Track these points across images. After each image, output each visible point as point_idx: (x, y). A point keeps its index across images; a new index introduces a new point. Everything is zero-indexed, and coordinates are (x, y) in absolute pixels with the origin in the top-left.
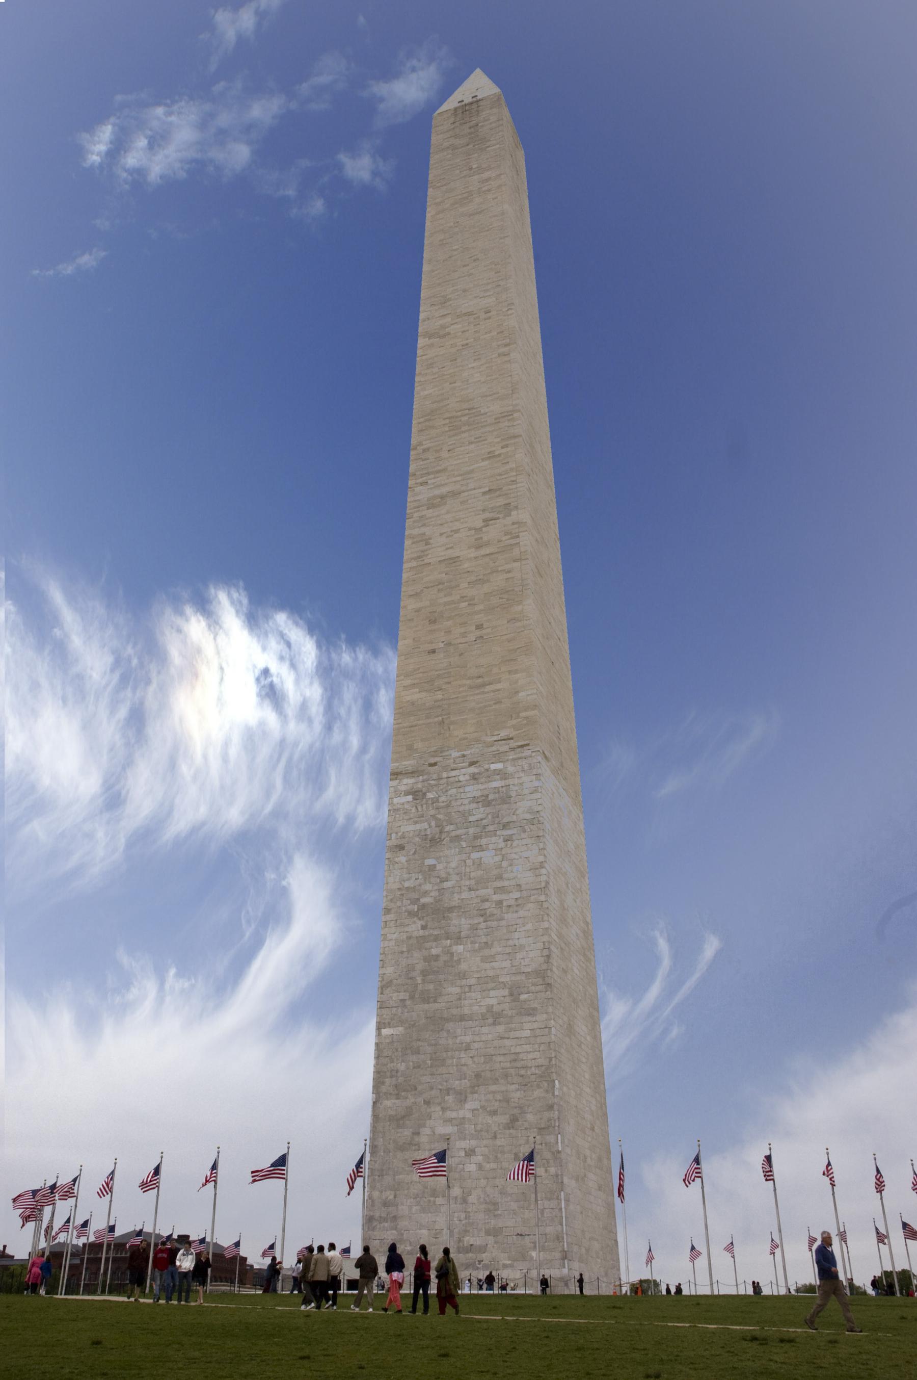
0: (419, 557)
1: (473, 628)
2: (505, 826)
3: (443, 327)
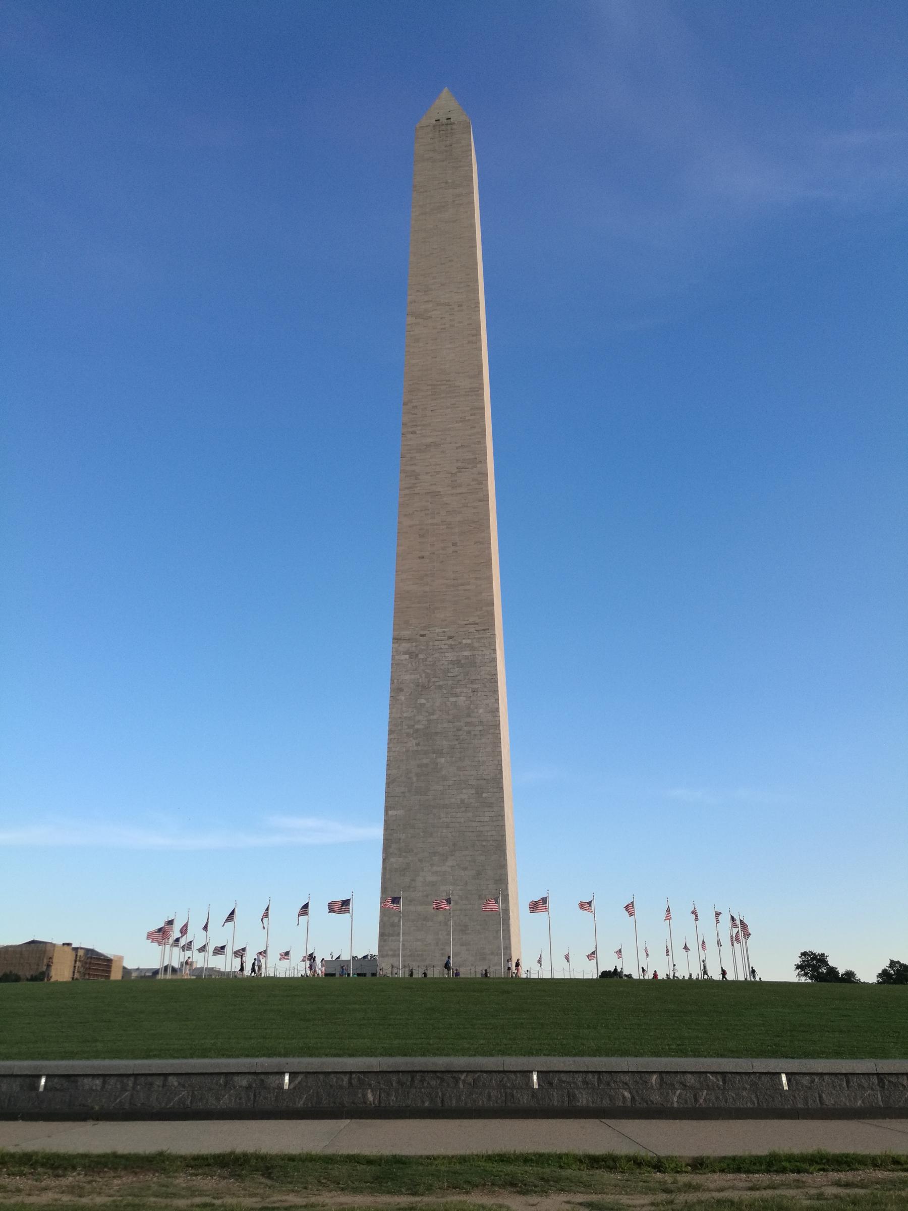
0: (410, 488)
1: (450, 544)
2: (473, 682)
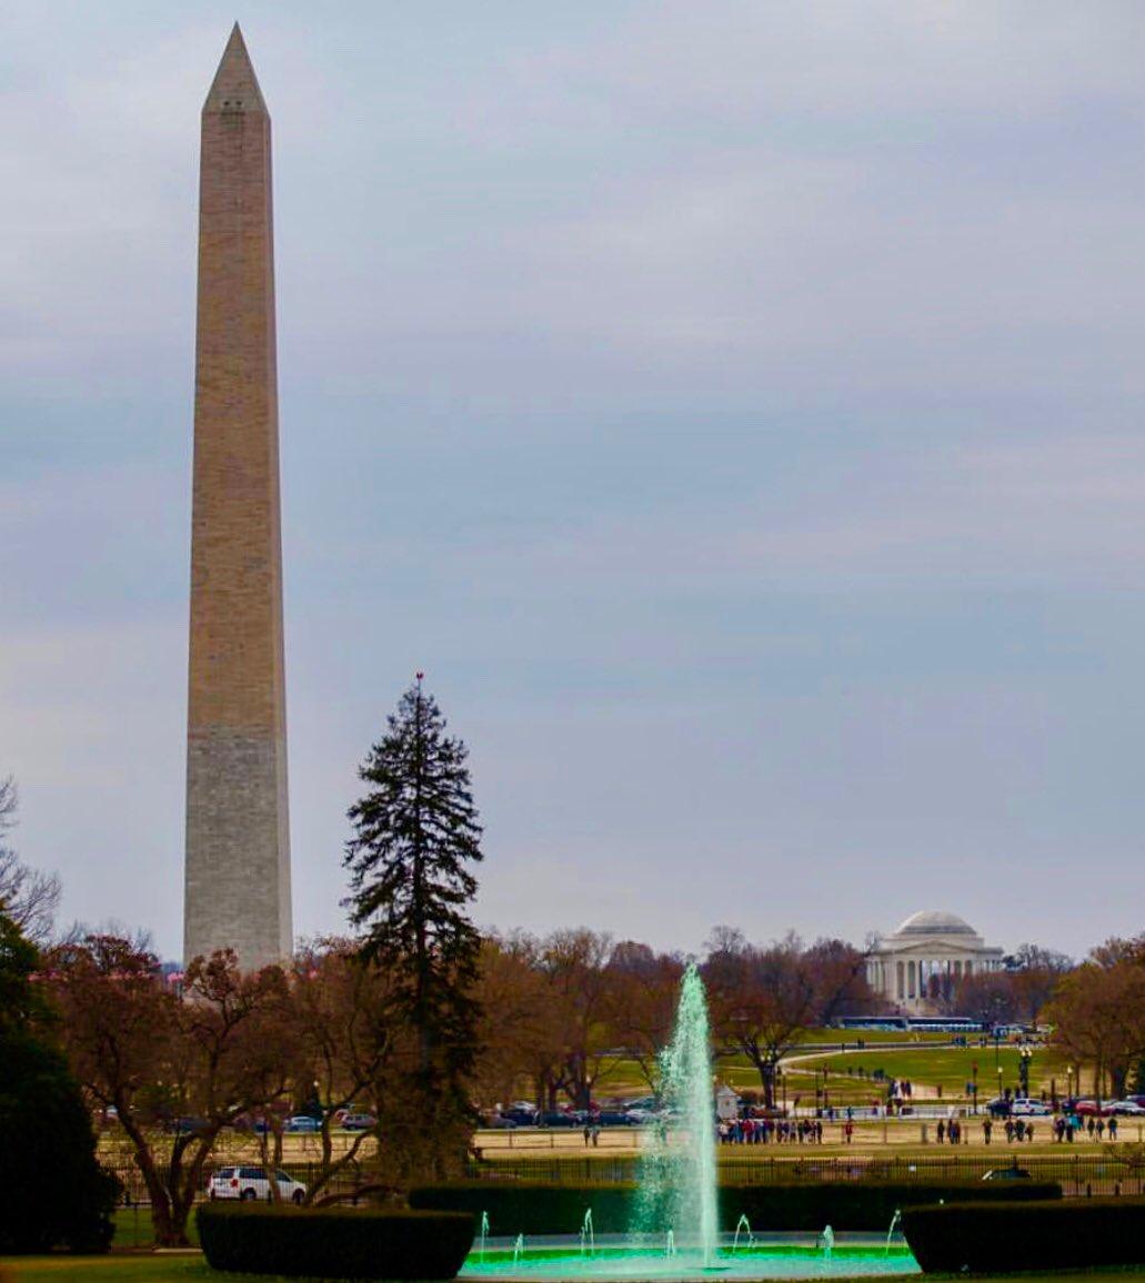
2: (257, 777)
3: (215, 379)
